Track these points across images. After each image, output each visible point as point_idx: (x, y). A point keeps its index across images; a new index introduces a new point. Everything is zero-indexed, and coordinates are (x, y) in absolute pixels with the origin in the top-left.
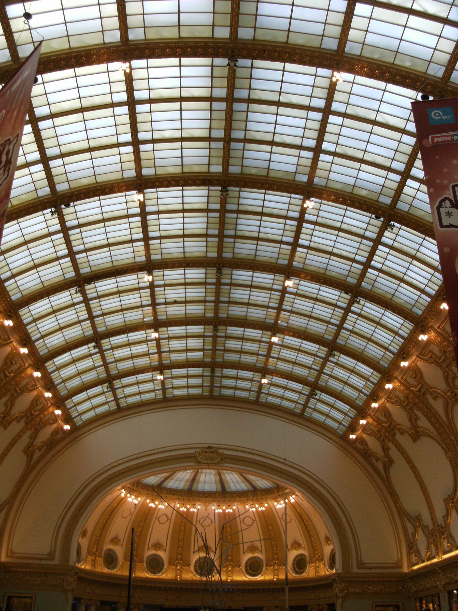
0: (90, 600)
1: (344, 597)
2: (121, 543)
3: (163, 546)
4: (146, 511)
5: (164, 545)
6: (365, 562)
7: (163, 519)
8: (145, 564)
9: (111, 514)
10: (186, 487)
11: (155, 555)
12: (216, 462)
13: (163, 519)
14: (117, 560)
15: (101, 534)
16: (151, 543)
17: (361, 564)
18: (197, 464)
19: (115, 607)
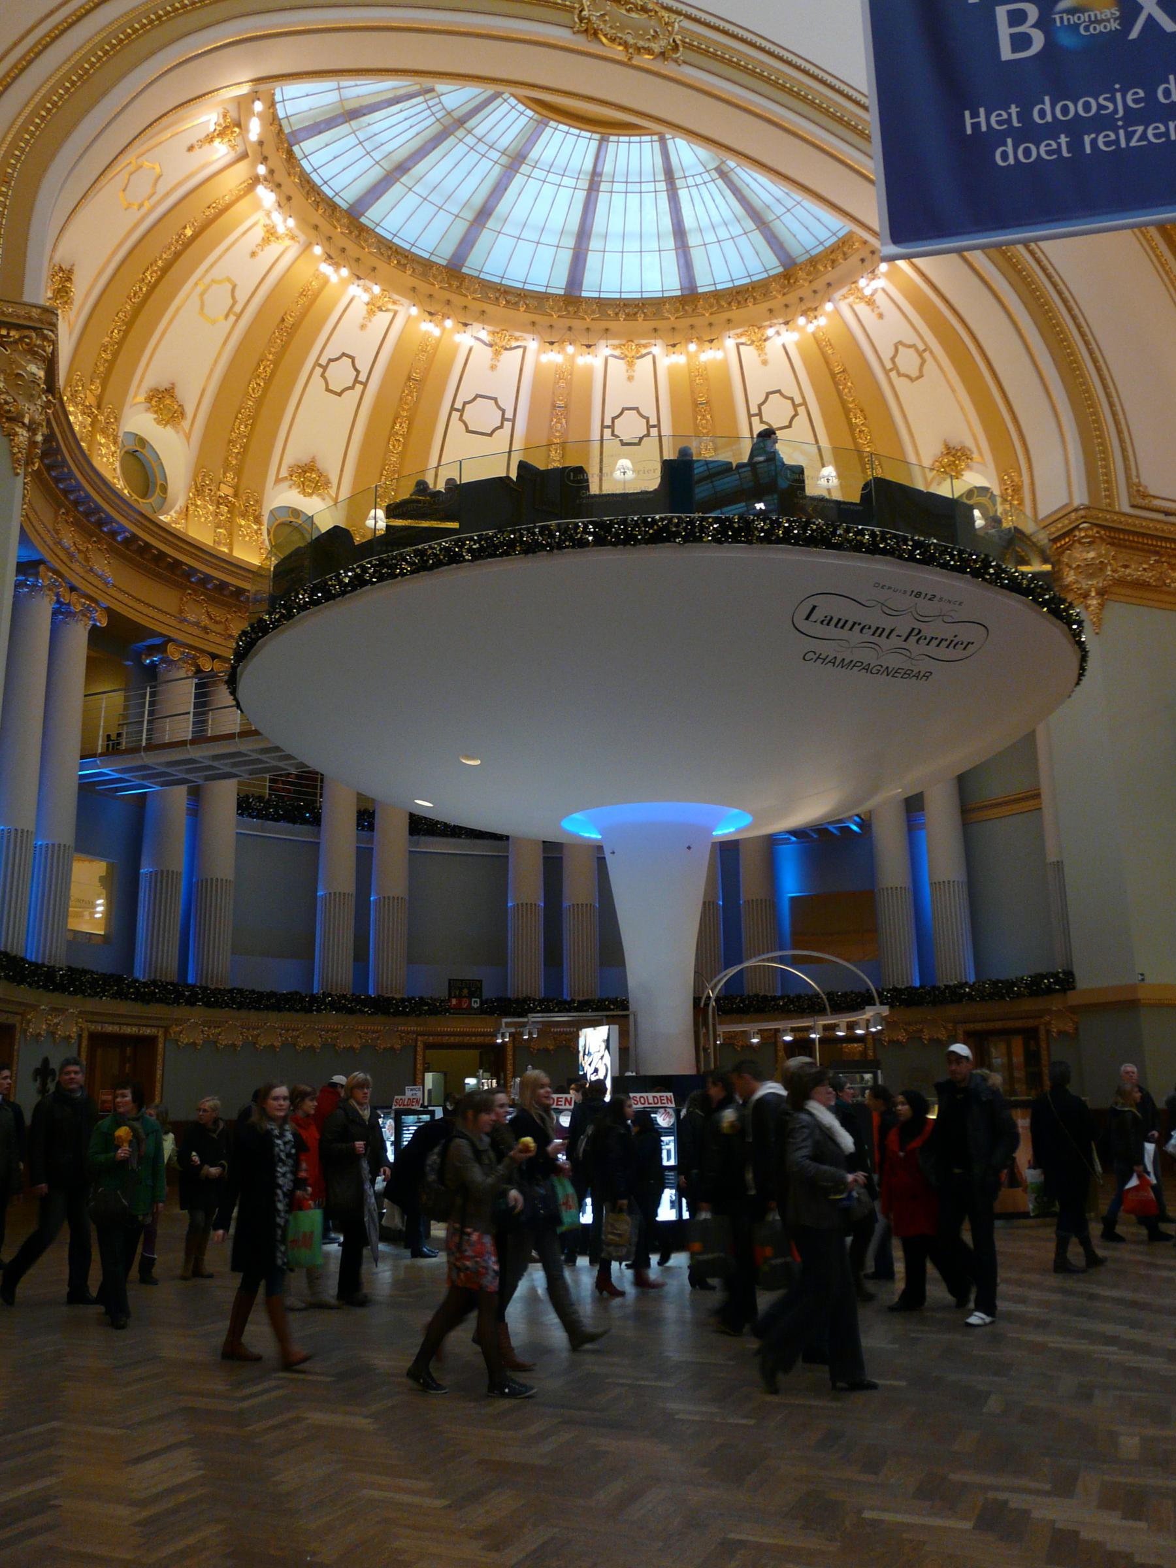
0: (73, 589)
1: (1101, 593)
2: (186, 424)
3: (327, 483)
4: (290, 320)
5: (334, 478)
6: (1152, 492)
7: (341, 374)
8: (264, 528)
9: (165, 270)
10: (443, 255)
11: (296, 512)
12: (656, 47)
13: (341, 374)
14: (164, 489)
15: (120, 343)
16: (289, 460)
17: (1139, 496)
18: (581, 42)
19: (153, 665)
